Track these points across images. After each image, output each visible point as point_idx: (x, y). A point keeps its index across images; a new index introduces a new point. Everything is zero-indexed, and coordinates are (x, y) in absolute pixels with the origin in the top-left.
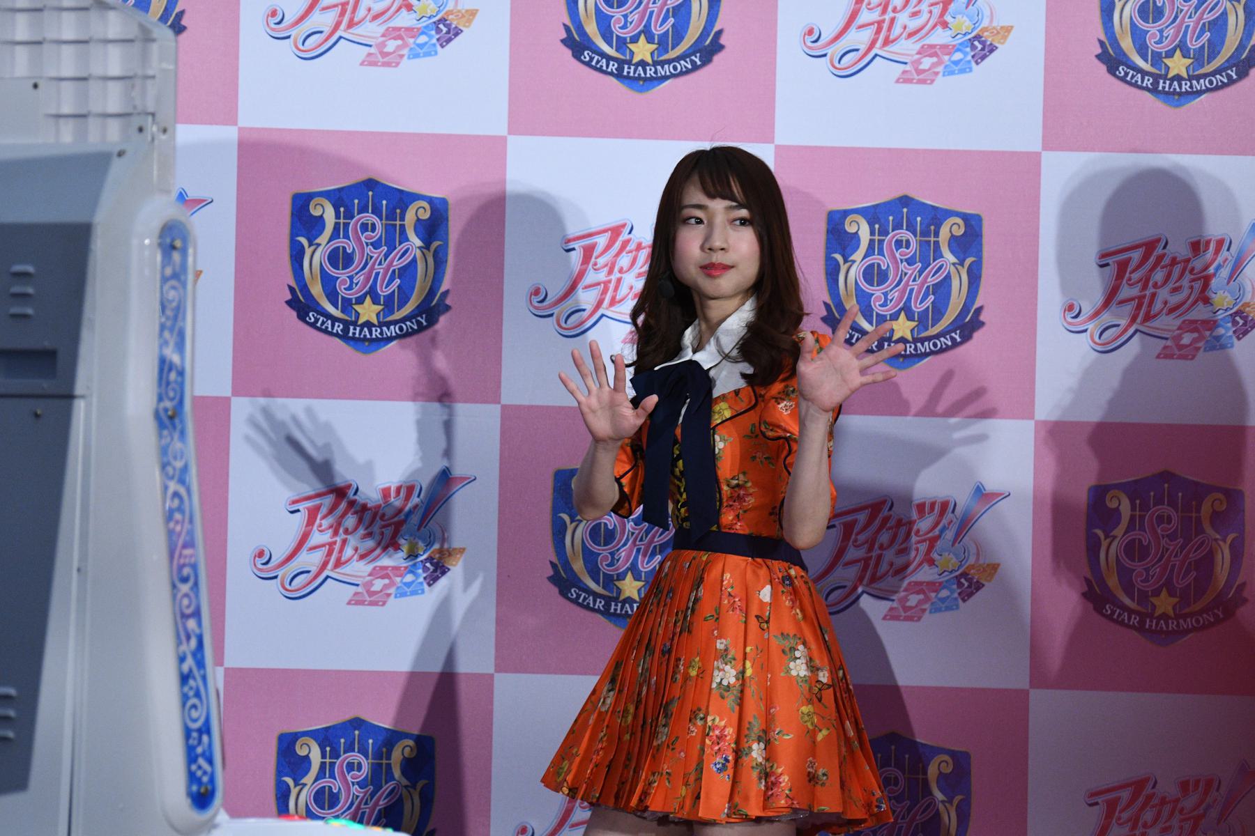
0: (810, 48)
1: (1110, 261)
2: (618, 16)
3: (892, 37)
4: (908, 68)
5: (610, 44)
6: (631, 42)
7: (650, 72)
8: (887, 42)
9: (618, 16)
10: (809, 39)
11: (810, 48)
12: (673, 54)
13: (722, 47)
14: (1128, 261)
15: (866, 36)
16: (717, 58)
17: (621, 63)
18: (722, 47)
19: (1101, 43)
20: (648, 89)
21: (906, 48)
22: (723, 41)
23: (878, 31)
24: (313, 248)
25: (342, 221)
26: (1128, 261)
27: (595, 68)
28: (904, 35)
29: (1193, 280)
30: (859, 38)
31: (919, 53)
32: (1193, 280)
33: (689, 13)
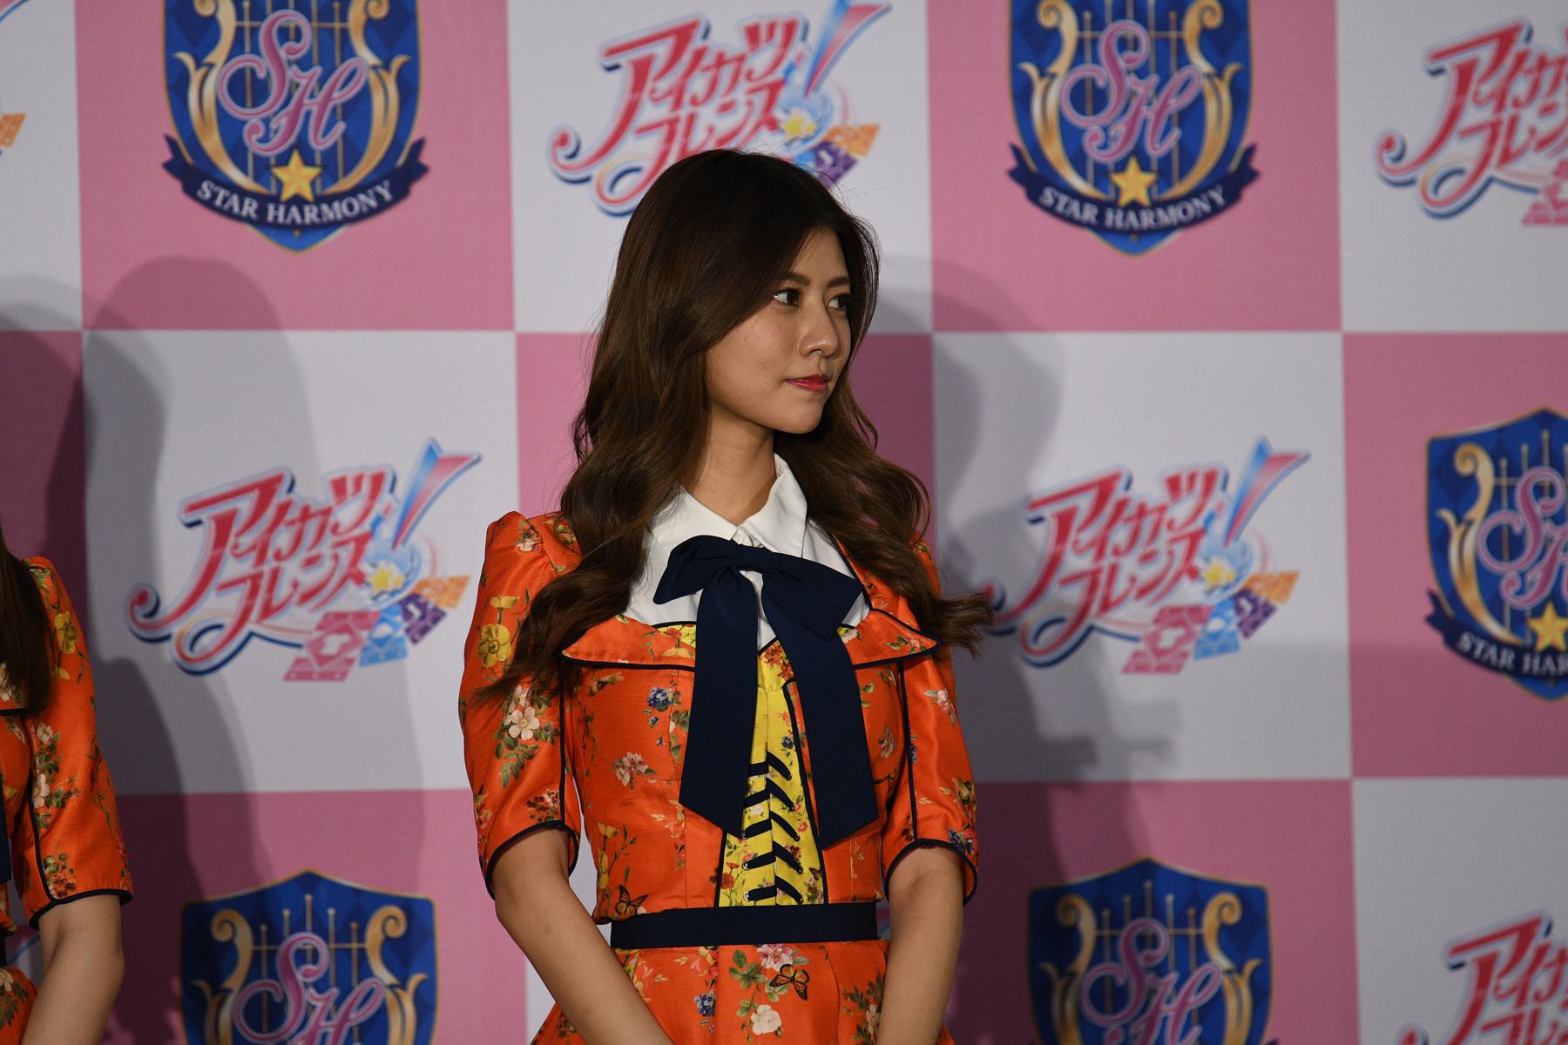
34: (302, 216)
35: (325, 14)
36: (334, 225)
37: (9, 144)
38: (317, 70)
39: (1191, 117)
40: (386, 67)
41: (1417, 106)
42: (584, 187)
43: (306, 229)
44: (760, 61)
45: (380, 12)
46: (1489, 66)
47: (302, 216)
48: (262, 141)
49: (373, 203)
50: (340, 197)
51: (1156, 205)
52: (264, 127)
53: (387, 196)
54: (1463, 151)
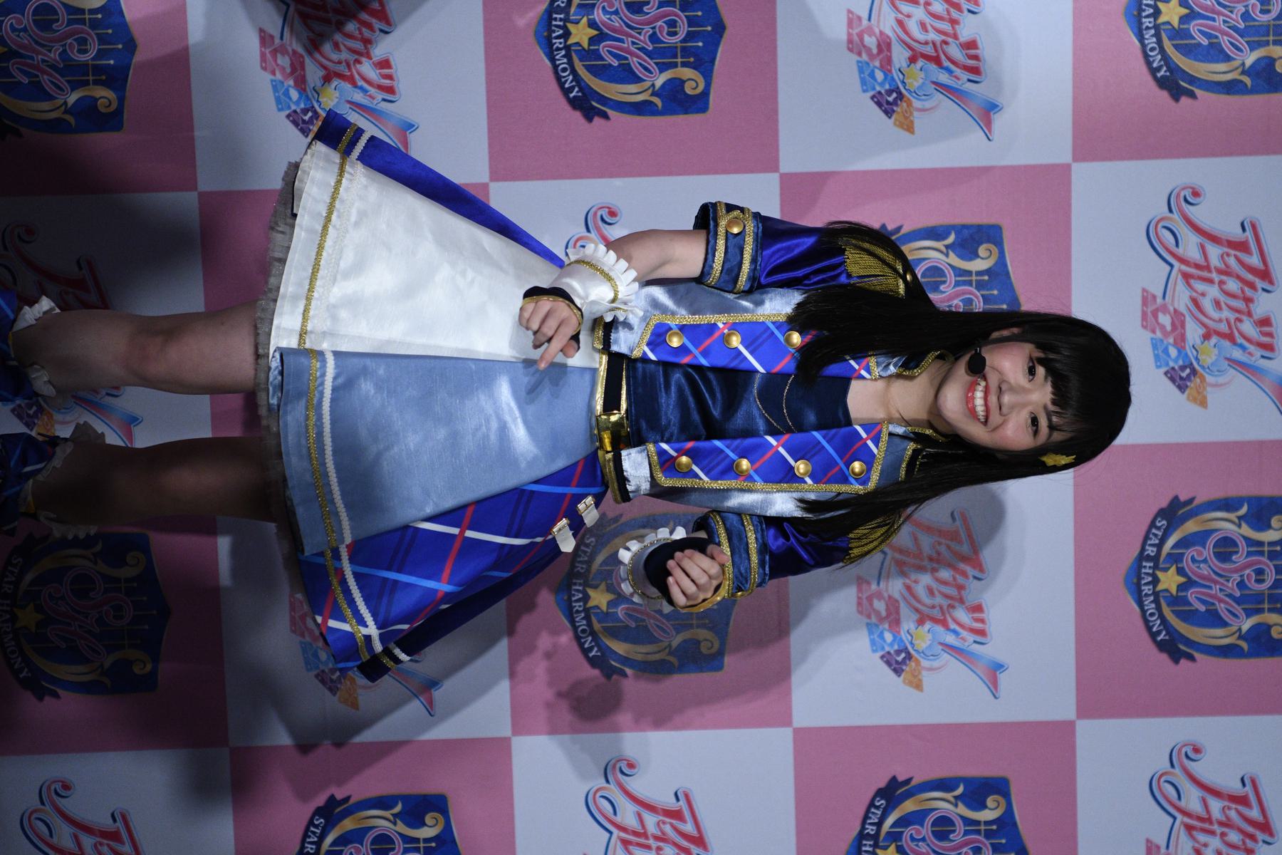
0: (1180, 750)
1: (958, 523)
2: (1205, 553)
3: (1194, 833)
4: (1159, 300)
5: (1176, 546)
6: (1178, 569)
7: (1147, 22)
8: (1189, 828)
9: (1205, 553)
10: (1188, 193)
11: (1178, 195)
12: (1167, 45)
13: (1176, 661)
14: (960, 542)
15: (1193, 253)
16: (1164, 657)
17: (1155, 559)
18: (1176, 661)
19: (1191, 501)
20: (1129, 589)
21: (1181, 298)
22: (1183, 661)
23: (1197, 266)
24: (944, 249)
25: (974, 278)
26: (960, 542)
27: (1148, 531)
28: (1194, 295)
29: (941, 608)
30: (1190, 246)
31: (1175, 311)
32: (941, 608)
33: (1217, 61)
34: (1147, 16)
35: (1272, 598)
36: (1140, 604)
37: (1188, 399)
38: (1242, 25)
39: (1214, 619)
40: (1240, 637)
41: (1221, 769)
42: (1168, 764)
43: (1139, 18)
44: (1248, 327)
45: (1275, 633)
46: (1246, 814)
47: (1147, 16)
48: (1193, 558)
49: (1155, 65)
50: (1159, 608)
51: (1156, 594)
52: (1202, 560)
53: (1159, 75)
54: (1193, 799)
